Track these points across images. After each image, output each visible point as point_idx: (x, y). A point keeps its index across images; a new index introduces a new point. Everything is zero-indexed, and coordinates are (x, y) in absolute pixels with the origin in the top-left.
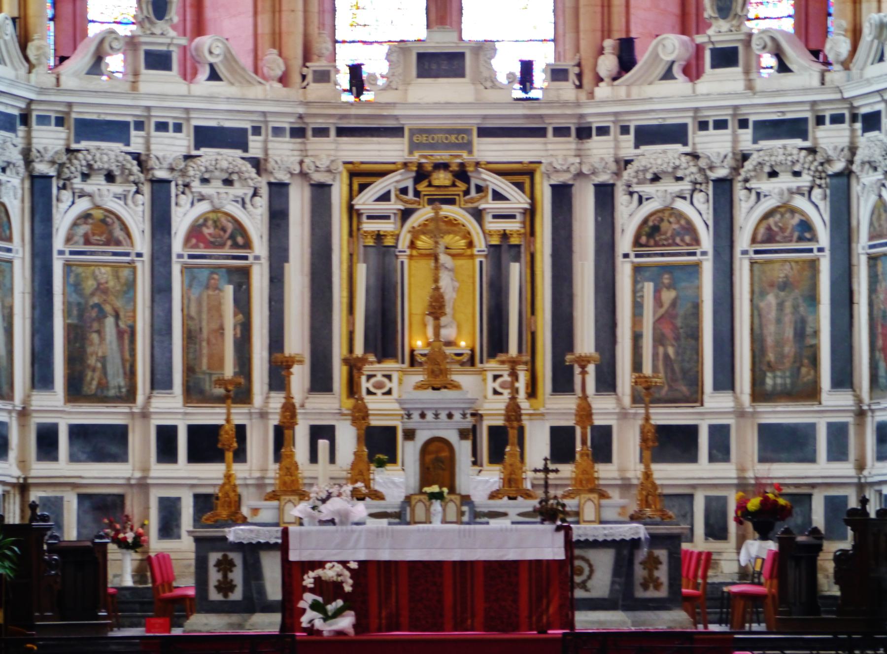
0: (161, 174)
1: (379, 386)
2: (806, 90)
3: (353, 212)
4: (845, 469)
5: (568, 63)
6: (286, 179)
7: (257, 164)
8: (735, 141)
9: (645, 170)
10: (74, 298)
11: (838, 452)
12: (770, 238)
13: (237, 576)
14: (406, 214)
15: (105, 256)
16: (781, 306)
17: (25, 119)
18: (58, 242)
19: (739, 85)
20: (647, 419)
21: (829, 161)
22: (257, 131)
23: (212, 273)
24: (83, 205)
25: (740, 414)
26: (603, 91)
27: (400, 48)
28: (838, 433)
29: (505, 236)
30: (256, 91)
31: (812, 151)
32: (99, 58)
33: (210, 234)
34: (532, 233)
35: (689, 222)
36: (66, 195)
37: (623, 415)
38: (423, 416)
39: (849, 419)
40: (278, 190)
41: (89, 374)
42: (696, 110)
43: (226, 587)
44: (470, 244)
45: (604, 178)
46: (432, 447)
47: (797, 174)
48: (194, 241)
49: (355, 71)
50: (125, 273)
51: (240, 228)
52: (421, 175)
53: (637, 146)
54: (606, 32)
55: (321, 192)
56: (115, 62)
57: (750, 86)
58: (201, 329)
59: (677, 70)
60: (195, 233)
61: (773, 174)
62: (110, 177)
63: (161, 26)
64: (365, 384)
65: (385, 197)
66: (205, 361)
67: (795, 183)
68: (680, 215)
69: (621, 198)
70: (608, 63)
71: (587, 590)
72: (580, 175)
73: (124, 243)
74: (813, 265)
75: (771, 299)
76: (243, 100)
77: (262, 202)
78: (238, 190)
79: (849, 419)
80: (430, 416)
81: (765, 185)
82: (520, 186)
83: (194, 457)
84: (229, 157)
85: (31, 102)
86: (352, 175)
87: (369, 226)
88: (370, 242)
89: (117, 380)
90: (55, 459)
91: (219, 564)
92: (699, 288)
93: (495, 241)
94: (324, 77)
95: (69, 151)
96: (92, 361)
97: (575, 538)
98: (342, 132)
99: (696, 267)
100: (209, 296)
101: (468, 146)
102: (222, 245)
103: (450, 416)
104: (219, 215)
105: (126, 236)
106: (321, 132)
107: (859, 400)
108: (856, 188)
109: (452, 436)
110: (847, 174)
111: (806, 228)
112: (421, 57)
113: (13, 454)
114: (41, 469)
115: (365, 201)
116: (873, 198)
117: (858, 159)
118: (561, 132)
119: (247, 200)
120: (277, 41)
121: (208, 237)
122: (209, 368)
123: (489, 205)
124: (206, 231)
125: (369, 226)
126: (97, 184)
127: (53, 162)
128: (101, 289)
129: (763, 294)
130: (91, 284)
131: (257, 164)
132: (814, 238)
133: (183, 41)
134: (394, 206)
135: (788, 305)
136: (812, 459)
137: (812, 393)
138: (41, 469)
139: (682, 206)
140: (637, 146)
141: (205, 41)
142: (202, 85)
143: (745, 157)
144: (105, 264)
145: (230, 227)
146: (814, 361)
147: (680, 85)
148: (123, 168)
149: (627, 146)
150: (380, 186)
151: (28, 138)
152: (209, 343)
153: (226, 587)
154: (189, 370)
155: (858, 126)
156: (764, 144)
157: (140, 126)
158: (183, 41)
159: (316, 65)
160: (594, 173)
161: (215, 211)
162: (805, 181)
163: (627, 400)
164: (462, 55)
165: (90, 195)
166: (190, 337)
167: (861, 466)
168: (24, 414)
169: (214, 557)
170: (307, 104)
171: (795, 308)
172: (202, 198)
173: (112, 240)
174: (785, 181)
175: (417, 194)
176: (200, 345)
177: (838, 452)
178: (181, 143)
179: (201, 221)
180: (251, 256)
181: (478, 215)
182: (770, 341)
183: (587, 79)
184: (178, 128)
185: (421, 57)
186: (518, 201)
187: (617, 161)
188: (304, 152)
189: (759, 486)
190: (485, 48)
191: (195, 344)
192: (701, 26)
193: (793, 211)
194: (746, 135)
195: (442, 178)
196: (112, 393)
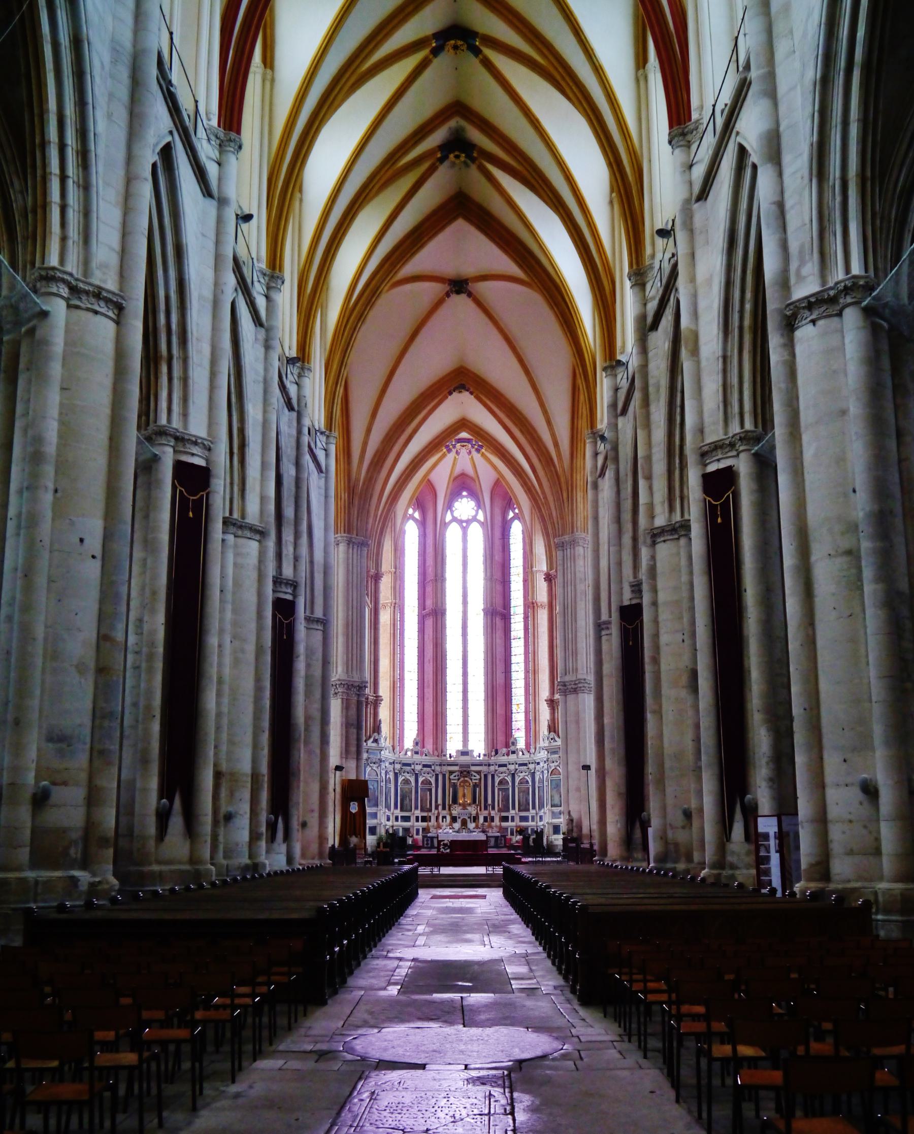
4: (534, 823)
7: (433, 771)
12: (521, 783)
13: (429, 842)
14: (459, 779)
15: (407, 787)
18: (399, 784)
24: (403, 778)
25: (516, 814)
26: (492, 758)
27: (457, 751)
28: (533, 818)
30: (433, 758)
37: (496, 814)
40: (437, 776)
51: (430, 782)
52: (461, 772)
55: (444, 776)
56: (409, 753)
60: (422, 782)
69: (496, 777)
70: (493, 753)
74: (529, 788)
77: (434, 777)
78: (430, 775)
81: (520, 774)
83: (422, 821)
84: (428, 769)
89: (409, 808)
94: (445, 755)
98: (448, 765)
106: (444, 765)
110: (534, 772)
111: (527, 782)
115: (452, 777)
118: (485, 765)
120: (437, 749)
123: (473, 778)
126: (406, 774)
131: (433, 771)
137: (528, 810)
142: (424, 757)
147: (506, 757)
149: (497, 768)
150: (454, 774)
153: (427, 844)
154: (421, 806)
166: (421, 800)
168: (393, 814)
174: (524, 774)
181: (471, 779)
186: (478, 777)
189: (519, 826)
190: (472, 751)
192: (509, 747)
194: (517, 766)
195: (465, 773)
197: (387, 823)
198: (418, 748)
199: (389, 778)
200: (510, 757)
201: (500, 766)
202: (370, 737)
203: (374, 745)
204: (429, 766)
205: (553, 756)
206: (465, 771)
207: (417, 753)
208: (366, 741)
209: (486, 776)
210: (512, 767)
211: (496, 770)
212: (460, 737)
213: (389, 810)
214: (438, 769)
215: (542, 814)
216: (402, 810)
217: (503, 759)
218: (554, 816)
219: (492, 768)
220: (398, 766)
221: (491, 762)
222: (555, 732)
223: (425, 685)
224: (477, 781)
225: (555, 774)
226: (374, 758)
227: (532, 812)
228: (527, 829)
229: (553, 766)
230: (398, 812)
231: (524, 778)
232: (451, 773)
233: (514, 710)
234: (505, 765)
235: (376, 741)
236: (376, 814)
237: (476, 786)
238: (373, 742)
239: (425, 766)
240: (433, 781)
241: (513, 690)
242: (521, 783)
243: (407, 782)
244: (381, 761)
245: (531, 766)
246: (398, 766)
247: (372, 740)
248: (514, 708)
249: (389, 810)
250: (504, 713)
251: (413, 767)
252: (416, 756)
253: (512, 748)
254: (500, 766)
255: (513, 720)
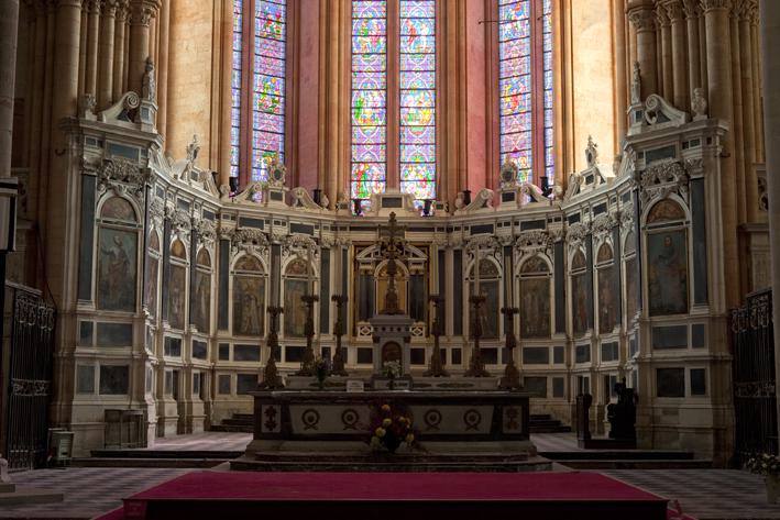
0: (276, 242)
1: (365, 332)
2: (545, 208)
3: (356, 262)
4: (562, 366)
5: (443, 202)
6: (329, 246)
7: (317, 241)
8: (513, 231)
9: (475, 244)
10: (238, 292)
11: (559, 359)
12: (528, 270)
13: (277, 418)
14: (377, 263)
15: (252, 274)
16: (533, 297)
17: (218, 216)
18: (231, 268)
19: (516, 208)
20: (477, 346)
21: (554, 237)
22: (317, 227)
24: (242, 253)
26: (457, 213)
28: (559, 352)
29: (417, 271)
30: (317, 211)
31: (547, 233)
32: (251, 194)
34: (428, 270)
35: (493, 264)
36: (235, 249)
37: (465, 344)
38: (384, 329)
39: (564, 345)
40: (325, 251)
41: (243, 324)
42: (497, 218)
43: (271, 425)
44: (403, 275)
45: (458, 247)
46: (387, 347)
47: (540, 243)
49: (357, 202)
50: (260, 282)
53: (472, 234)
54: (459, 190)
57: (519, 207)
59: (488, 203)
60: (290, 267)
61: (530, 244)
62: (255, 243)
63: (278, 183)
64: (359, 331)
65: (369, 255)
67: (539, 247)
68: (490, 262)
69: (465, 256)
70: (459, 202)
71: (476, 429)
72: (447, 247)
74: (548, 281)
75: (529, 296)
76: (310, 213)
79: (564, 345)
80: (388, 330)
81: (527, 249)
82: (424, 251)
85: (220, 208)
86: (355, 247)
87: (362, 267)
88: (362, 273)
90: (228, 359)
91: (267, 412)
92: (497, 292)
93: (413, 273)
95: (237, 230)
96: (245, 318)
97: (532, 413)
98: (351, 229)
99: (497, 283)
101: (403, 235)
103: (399, 329)
106: (344, 229)
107: (568, 338)
108: (566, 247)
109: (400, 341)
110: (562, 242)
111: (544, 266)
112: (384, 199)
113: (209, 359)
114: (220, 363)
115: (361, 257)
116: (575, 251)
117: (568, 235)
118: (440, 229)
120: (327, 194)
123: (411, 259)
125: (362, 267)
126: (249, 245)
127: (229, 234)
128: (249, 288)
129: (525, 294)
130: (245, 286)
131: (317, 241)
132: (548, 270)
133: (287, 189)
134: (372, 259)
135: (536, 299)
136: (547, 363)
138: (220, 363)
139: (490, 258)
140: (472, 234)
141: (299, 189)
143: (517, 237)
144: (250, 278)
146: (548, 321)
148: (259, 238)
149: (467, 234)
151: (219, 224)
153: (271, 425)
155: (567, 222)
156: (525, 231)
157: (268, 222)
158: (287, 189)
159: (341, 202)
160: (454, 245)
161: (299, 258)
162: (544, 245)
163: (467, 338)
164: (401, 199)
165: (246, 250)
167: (569, 365)
168: (214, 340)
169: (265, 408)
170: (337, 217)
171: (539, 299)
172: (293, 253)
173: (255, 268)
174: (535, 247)
175: (382, 254)
177: (559, 359)
178: (282, 231)
181: (406, 263)
182: (528, 313)
183: (450, 209)
184: (284, 224)
185: (384, 199)
186: (423, 258)
187: (463, 240)
188: (336, 237)
193: (539, 259)
194: (518, 229)
196: (253, 332)
197: (195, 361)
198: (278, 186)
199: (204, 250)
200: (499, 209)
201: (475, 230)
202: (114, 102)
203: (121, 124)
204: (308, 230)
205: (657, 163)
206: (391, 241)
207: (276, 197)
208: (98, 111)
209: (442, 254)
210: (505, 232)
211: (467, 242)
212: (378, 171)
213: (204, 328)
214: (328, 236)
215: (589, 342)
216: (237, 330)
217: (486, 214)
218: (663, 338)
219: (456, 236)
220: (228, 225)
221: (454, 222)
222: (659, 91)
223: (303, 50)
224: (421, 267)
225: (662, 217)
226: (121, 163)
227: (557, 339)
228: (542, 380)
229: (656, 193)
230: (227, 335)
231: (535, 258)
232: (359, 247)
233: (506, 111)
234: (489, 229)
235: (131, 114)
236: (131, 326)
237: (416, 277)
238: (120, 117)
239: (295, 228)
240: (316, 264)
241: (504, 65)
242: (527, 269)
243: (250, 263)
244: (147, 174)
245: (555, 228)
246: (228, 225)
247: (117, 109)
248: (506, 102)
249: (204, 328)
250: (483, 115)
251: (266, 229)
252: (273, 204)
253: (506, 186)
254: (475, 230)
255: (504, 130)
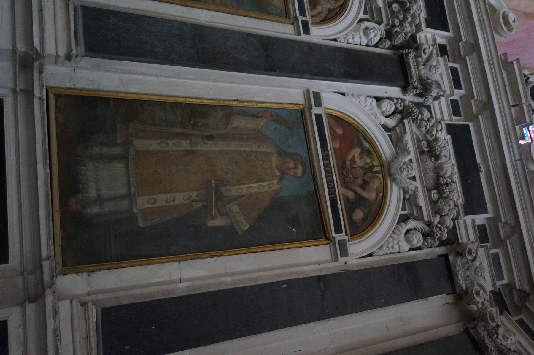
23: (303, 164)
33: (353, 160)
48: (340, 132)
58: (211, 138)
66: (153, 145)
73: (315, 12)
100: (268, 155)
102: (346, 184)
104: (380, 175)
105: (323, 16)
119: (412, 224)
121: (350, 157)
122: (137, 152)
124: (356, 152)
145: (371, 196)
152: (188, 152)
176: (183, 136)
179: (367, 145)
180: (341, 236)
191: (183, 125)
